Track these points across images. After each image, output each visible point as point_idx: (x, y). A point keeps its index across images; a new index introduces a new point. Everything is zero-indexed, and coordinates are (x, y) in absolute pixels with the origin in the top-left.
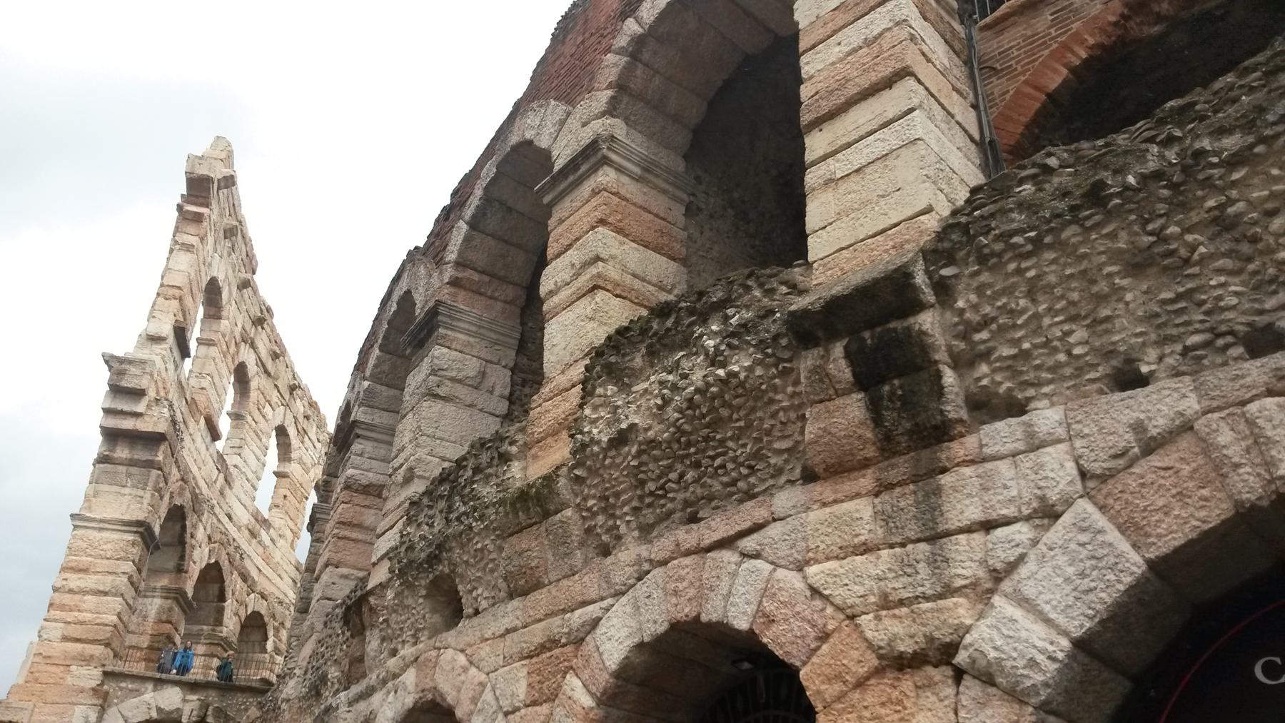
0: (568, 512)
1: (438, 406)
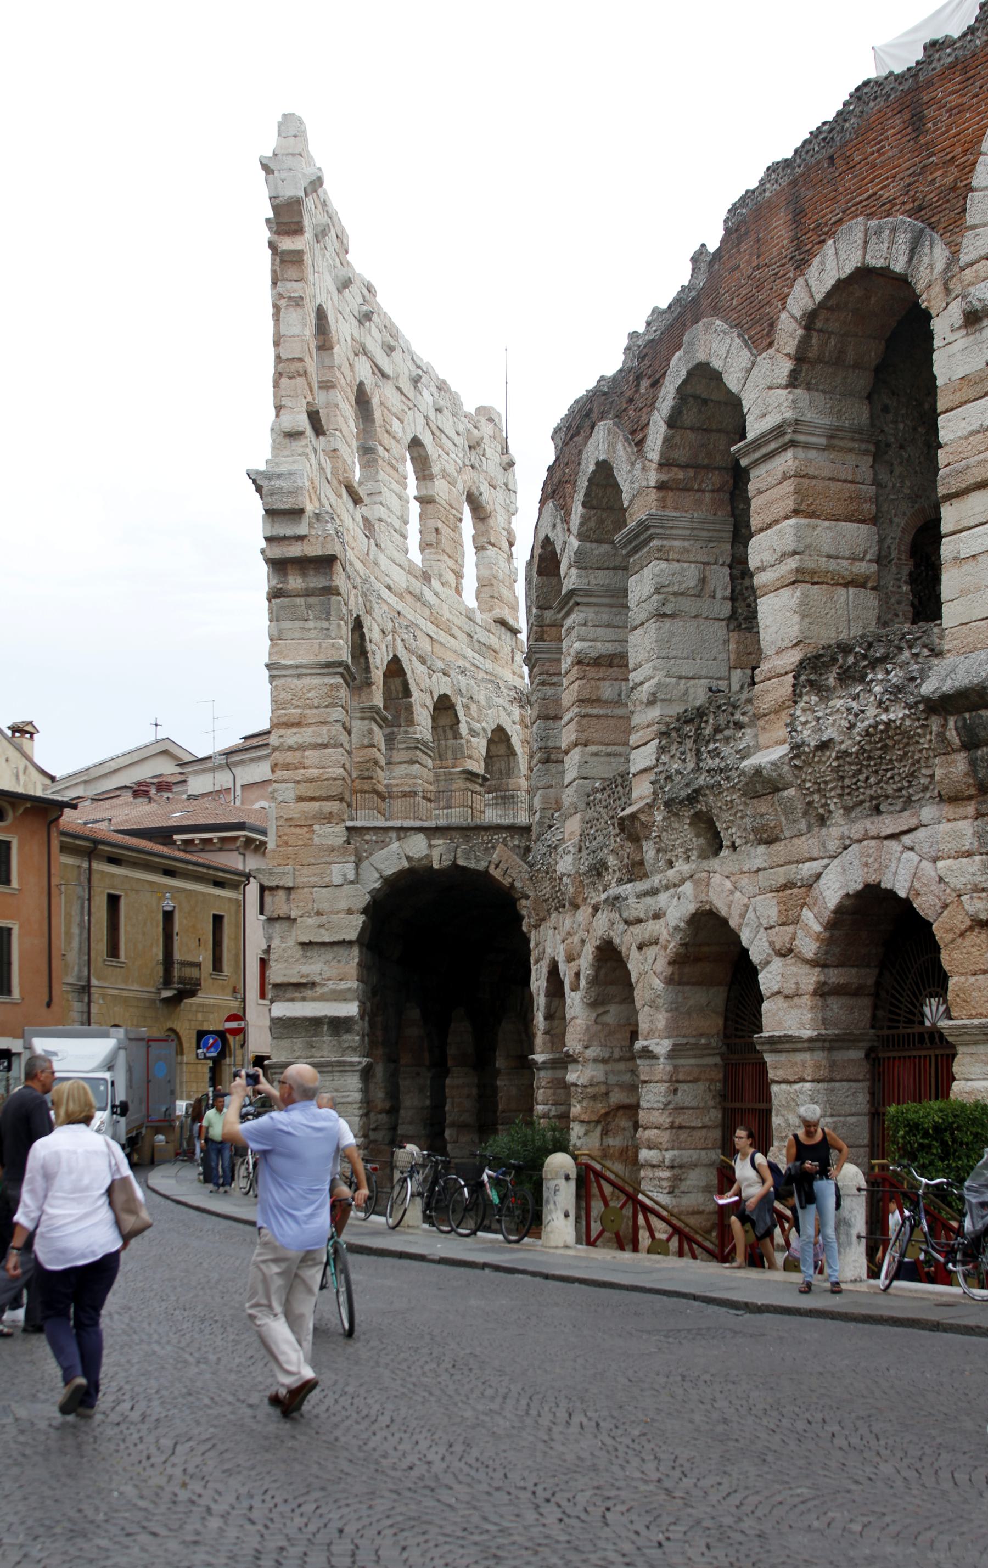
0: (792, 792)
1: (668, 624)
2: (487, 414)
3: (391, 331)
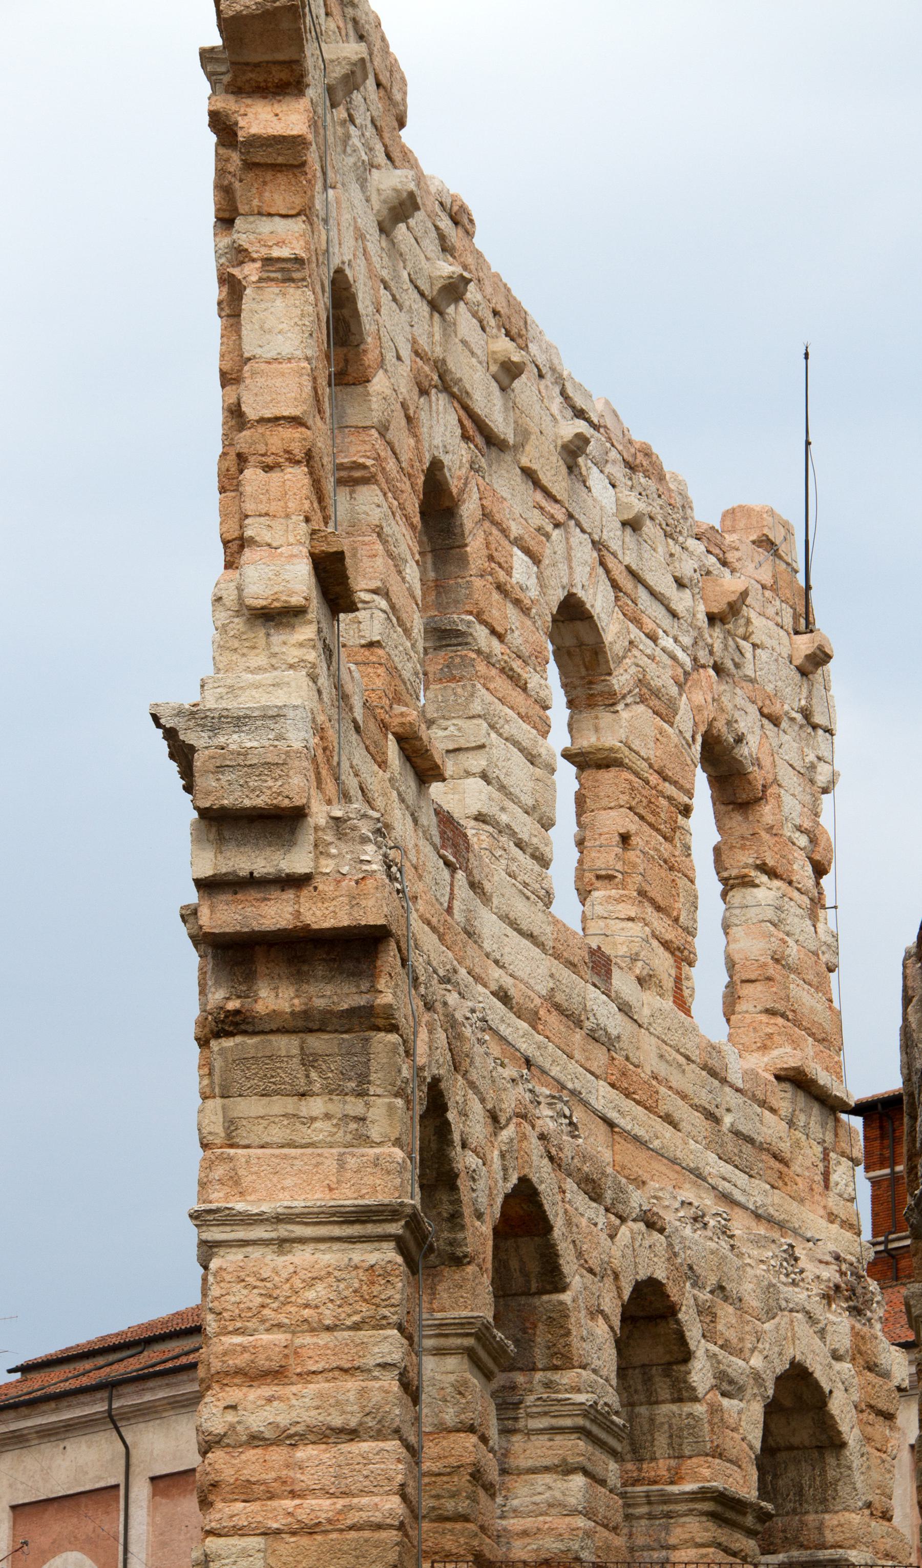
3: (511, 322)
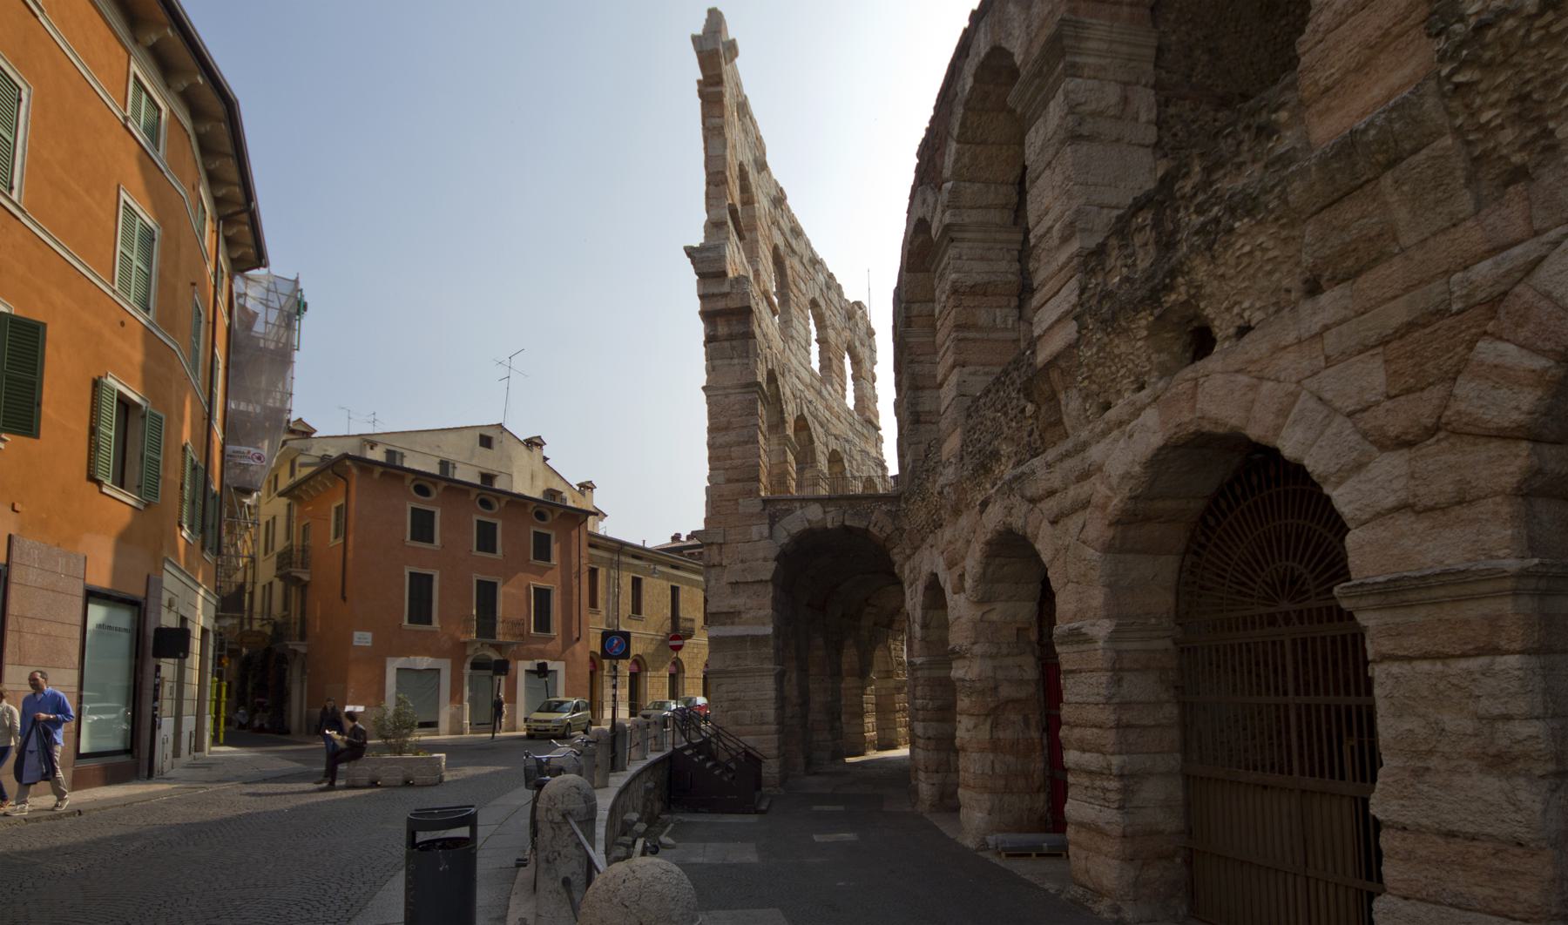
2: (859, 304)
